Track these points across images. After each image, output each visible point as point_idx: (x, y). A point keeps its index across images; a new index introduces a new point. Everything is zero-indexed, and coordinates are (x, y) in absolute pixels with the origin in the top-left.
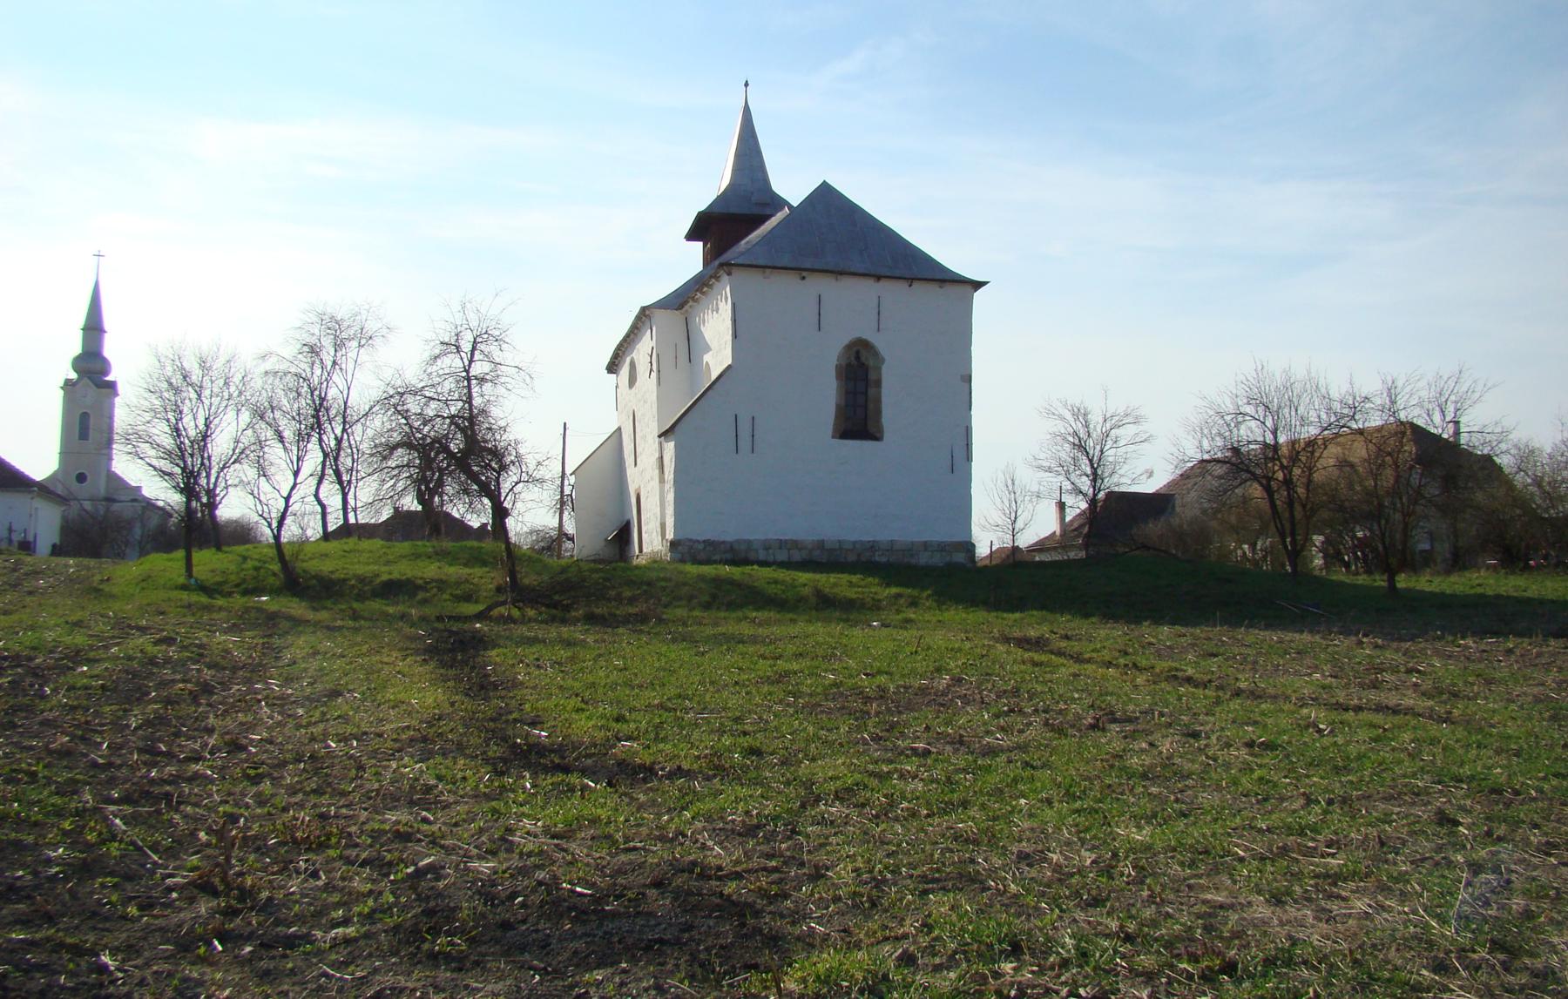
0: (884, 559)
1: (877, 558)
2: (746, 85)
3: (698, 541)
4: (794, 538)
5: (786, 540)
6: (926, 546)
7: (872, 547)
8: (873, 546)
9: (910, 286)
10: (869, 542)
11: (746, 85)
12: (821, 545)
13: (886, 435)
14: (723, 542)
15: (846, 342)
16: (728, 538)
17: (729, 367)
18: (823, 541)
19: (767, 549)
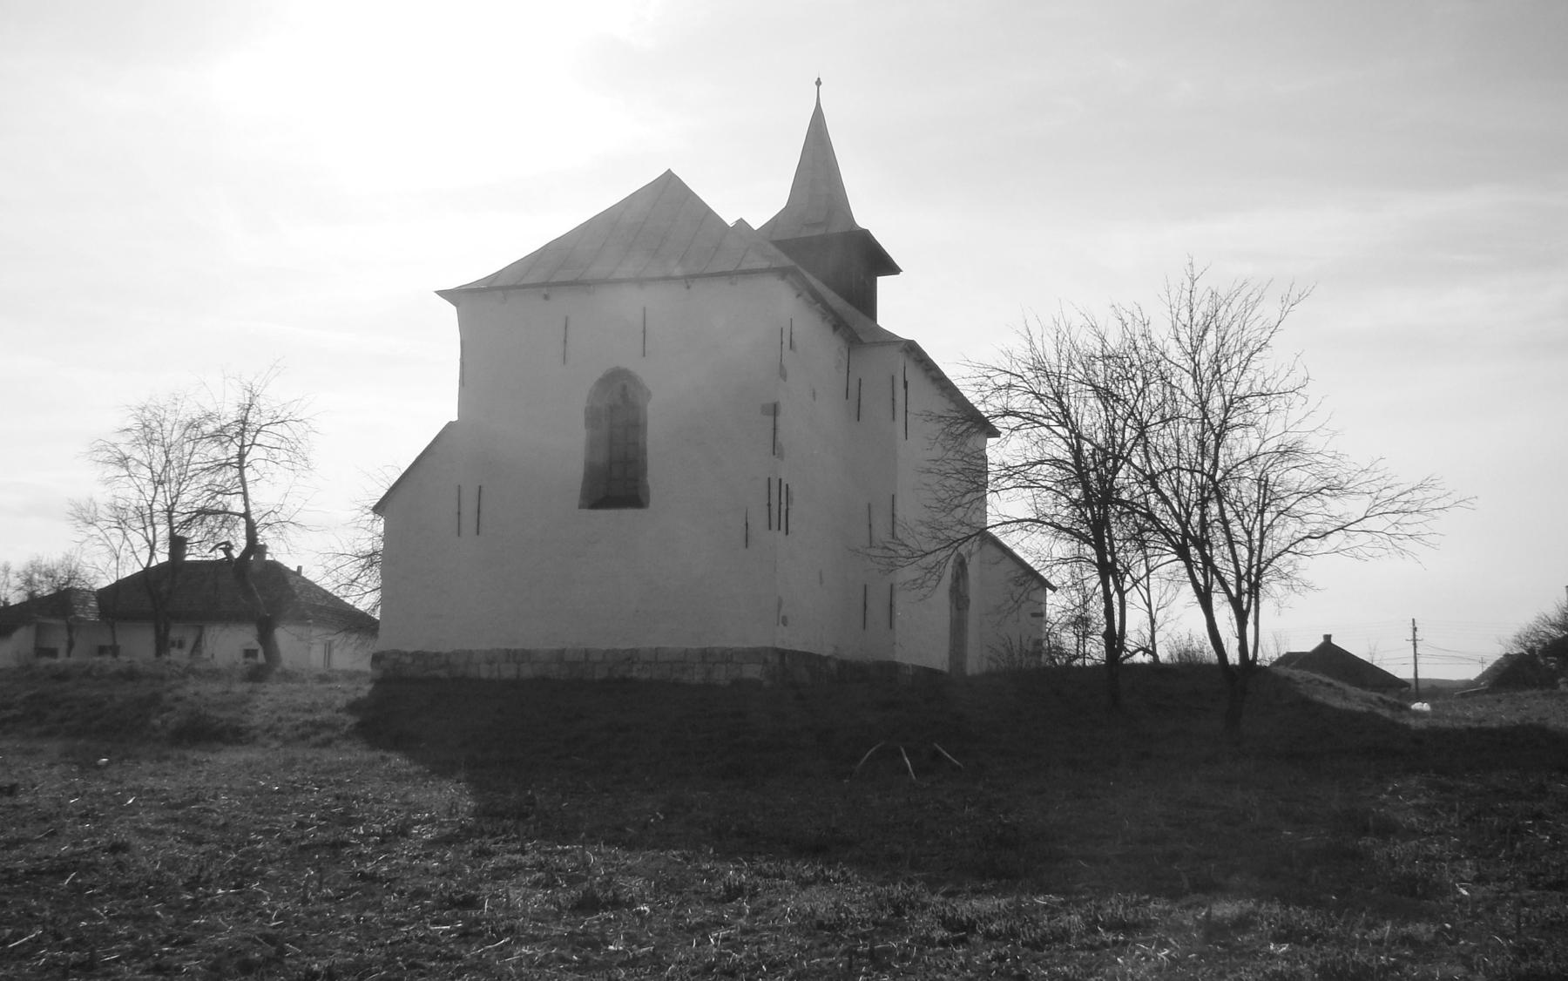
0: (645, 676)
1: (634, 674)
2: (818, 83)
3: (406, 654)
4: (527, 648)
5: (516, 651)
6: (705, 654)
7: (629, 659)
8: (631, 657)
9: (688, 287)
10: (624, 651)
11: (818, 83)
12: (560, 656)
13: (651, 504)
14: (437, 655)
15: (600, 375)
16: (446, 648)
17: (450, 425)
18: (563, 651)
19: (490, 663)
